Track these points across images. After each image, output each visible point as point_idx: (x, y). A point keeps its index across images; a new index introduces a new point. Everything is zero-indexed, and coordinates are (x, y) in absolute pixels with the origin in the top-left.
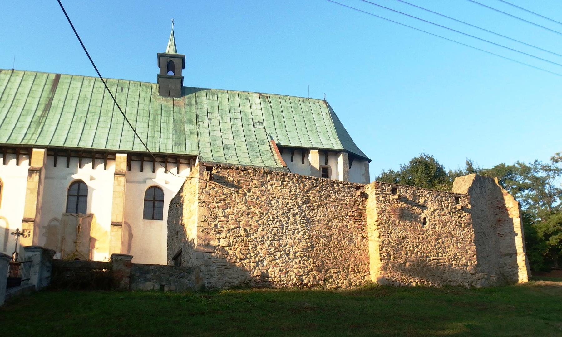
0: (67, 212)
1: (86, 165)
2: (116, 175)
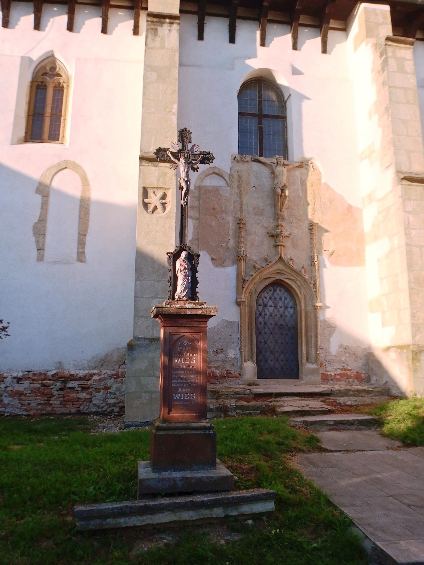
0: (240, 152)
1: (275, 39)
2: (390, 43)
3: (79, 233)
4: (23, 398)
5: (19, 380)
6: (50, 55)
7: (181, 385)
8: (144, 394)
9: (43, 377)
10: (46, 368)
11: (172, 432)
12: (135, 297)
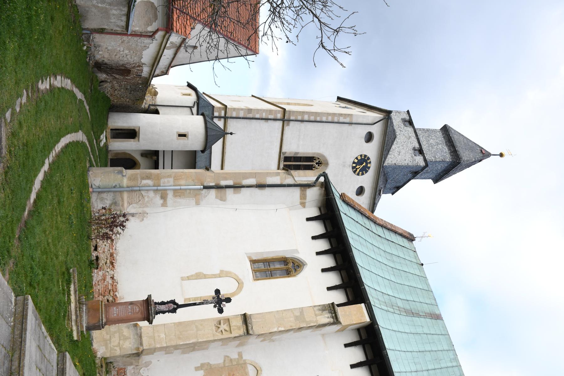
3: (201, 297)
4: (102, 281)
5: (112, 278)
6: (304, 264)
7: (119, 310)
8: (109, 336)
9: (115, 290)
10: (120, 291)
11: (100, 307)
12: (164, 324)
